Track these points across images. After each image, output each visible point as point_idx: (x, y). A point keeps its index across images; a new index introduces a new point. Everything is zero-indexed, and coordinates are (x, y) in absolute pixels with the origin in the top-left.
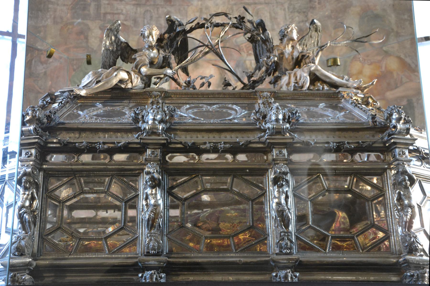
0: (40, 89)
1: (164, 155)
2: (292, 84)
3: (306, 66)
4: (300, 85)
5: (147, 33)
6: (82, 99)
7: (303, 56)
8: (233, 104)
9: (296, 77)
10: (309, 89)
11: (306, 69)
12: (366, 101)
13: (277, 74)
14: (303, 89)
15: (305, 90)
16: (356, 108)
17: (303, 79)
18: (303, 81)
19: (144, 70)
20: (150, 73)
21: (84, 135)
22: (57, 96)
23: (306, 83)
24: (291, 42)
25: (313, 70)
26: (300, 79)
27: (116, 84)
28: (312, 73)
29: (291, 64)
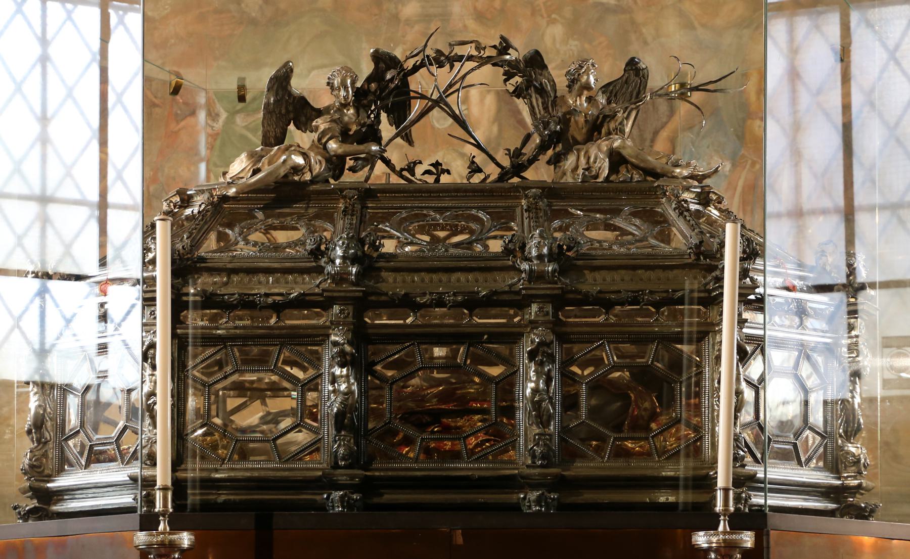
0: (156, 97)
1: (359, 315)
2: (580, 171)
3: (605, 140)
4: (594, 173)
5: (338, 83)
6: (231, 202)
7: (605, 117)
8: (479, 208)
9: (589, 158)
10: (607, 179)
11: (604, 145)
12: (705, 198)
13: (559, 148)
14: (597, 180)
15: (602, 182)
16: (681, 218)
17: (599, 163)
18: (599, 165)
19: (333, 145)
20: (343, 152)
21: (235, 278)
22: (191, 197)
23: (603, 170)
24: (585, 92)
25: (617, 148)
26: (595, 162)
27: (286, 176)
28: (615, 151)
29: (584, 130)
